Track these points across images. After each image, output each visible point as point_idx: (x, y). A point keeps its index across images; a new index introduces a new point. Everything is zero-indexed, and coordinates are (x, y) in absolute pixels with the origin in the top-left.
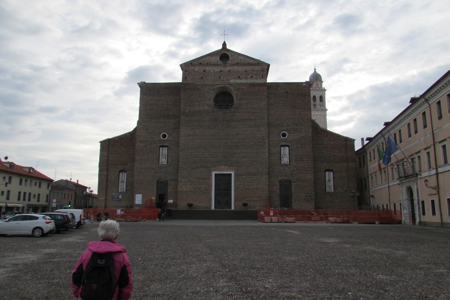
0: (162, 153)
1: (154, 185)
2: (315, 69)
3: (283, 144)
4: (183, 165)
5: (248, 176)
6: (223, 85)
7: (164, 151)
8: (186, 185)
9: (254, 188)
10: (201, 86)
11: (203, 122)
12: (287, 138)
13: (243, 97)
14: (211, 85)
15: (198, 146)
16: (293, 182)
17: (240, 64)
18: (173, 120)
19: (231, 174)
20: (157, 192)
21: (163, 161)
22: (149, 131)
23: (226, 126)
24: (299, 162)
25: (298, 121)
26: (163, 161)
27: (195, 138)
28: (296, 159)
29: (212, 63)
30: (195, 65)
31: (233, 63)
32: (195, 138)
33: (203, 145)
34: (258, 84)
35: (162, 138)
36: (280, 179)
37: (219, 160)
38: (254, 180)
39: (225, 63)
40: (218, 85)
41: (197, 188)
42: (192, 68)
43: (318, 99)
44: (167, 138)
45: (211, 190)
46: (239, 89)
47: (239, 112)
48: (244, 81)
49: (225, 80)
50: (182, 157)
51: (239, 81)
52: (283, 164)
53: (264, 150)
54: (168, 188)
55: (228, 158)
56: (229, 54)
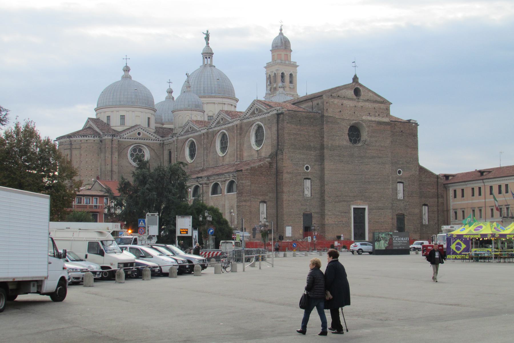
0: (306, 186)
1: (301, 218)
2: (281, 30)
3: (399, 180)
4: (329, 199)
5: (377, 210)
6: (358, 121)
7: (308, 183)
8: (331, 218)
9: (382, 221)
10: (340, 120)
11: (342, 157)
12: (402, 175)
13: (373, 134)
14: (348, 120)
15: (340, 180)
16: (406, 216)
17: (370, 101)
18: (314, 152)
19: (364, 209)
20: (303, 225)
21: (308, 193)
22: (294, 162)
23: (361, 162)
24: (410, 197)
25: (409, 159)
26: (308, 193)
27: (337, 173)
28: (408, 195)
29: (348, 97)
30: (333, 97)
31: (365, 99)
32: (337, 173)
33: (343, 180)
34: (384, 122)
35: (306, 170)
36: (397, 212)
37: (356, 195)
38: (381, 214)
39: (358, 98)
40: (353, 120)
41: (340, 221)
42: (332, 101)
43: (287, 79)
44: (310, 170)
45: (351, 223)
46: (370, 126)
47: (370, 149)
48: (373, 119)
49: (359, 115)
50: (327, 191)
51: (369, 118)
52: (399, 200)
53: (388, 186)
54: (313, 220)
55: (363, 193)
56: (361, 88)
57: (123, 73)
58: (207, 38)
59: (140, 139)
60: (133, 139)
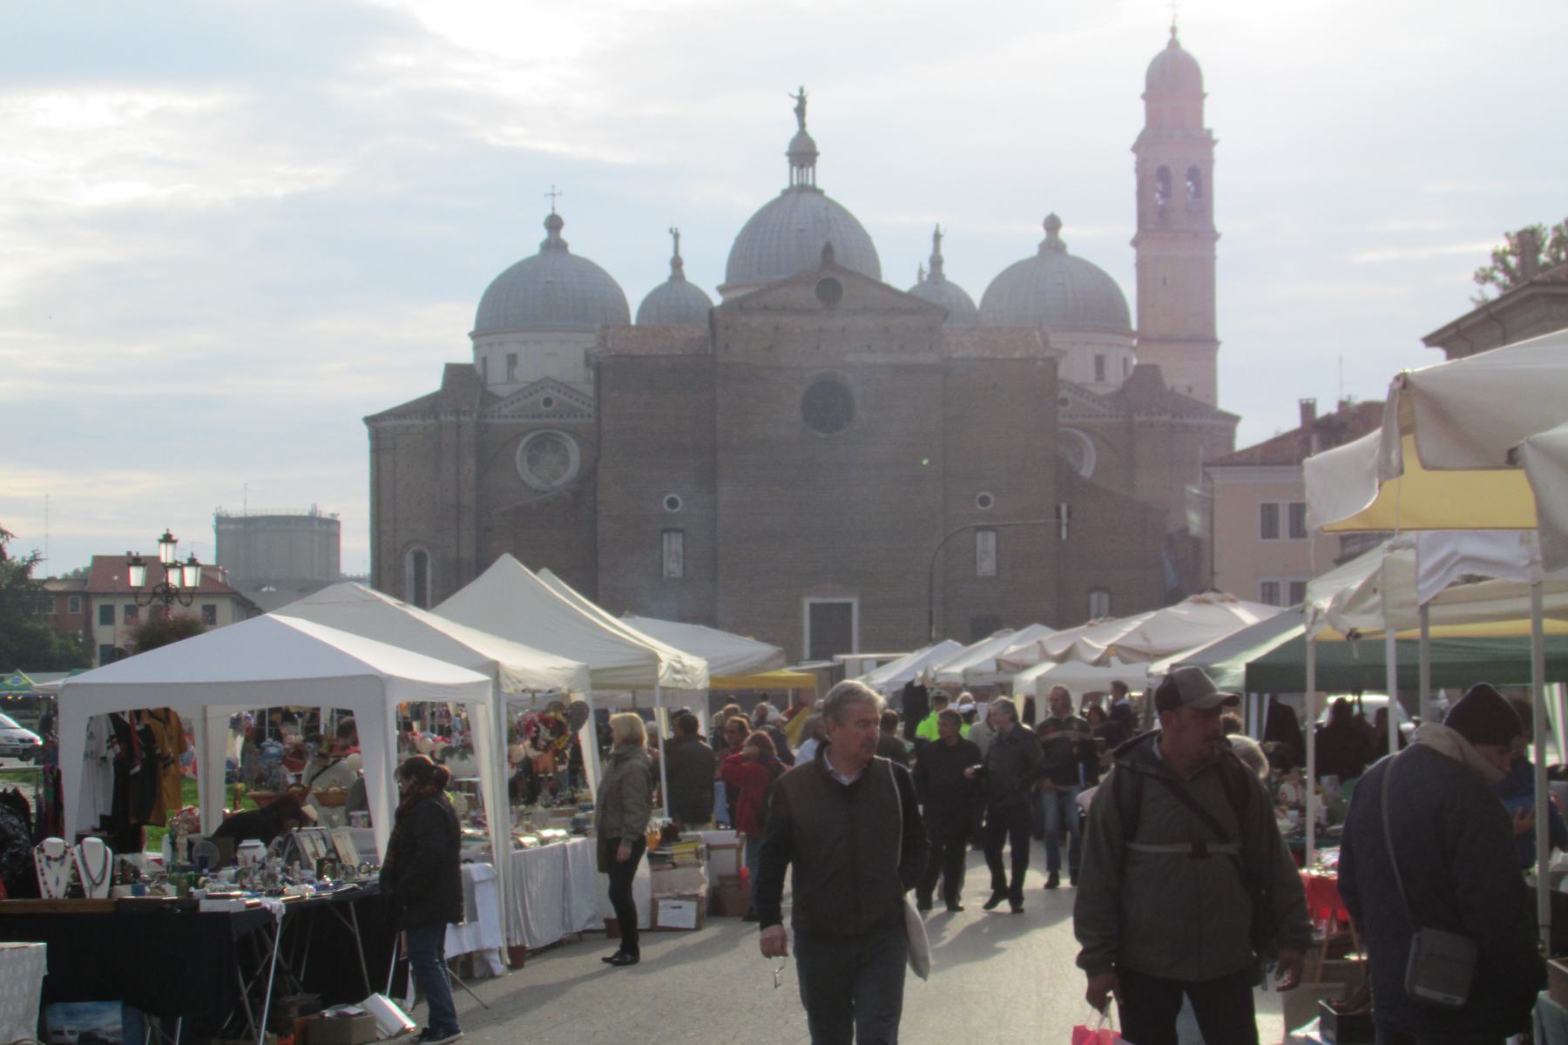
19: (848, 606)
56: (841, 280)
57: (543, 234)
58: (800, 111)
59: (547, 416)
60: (527, 416)
